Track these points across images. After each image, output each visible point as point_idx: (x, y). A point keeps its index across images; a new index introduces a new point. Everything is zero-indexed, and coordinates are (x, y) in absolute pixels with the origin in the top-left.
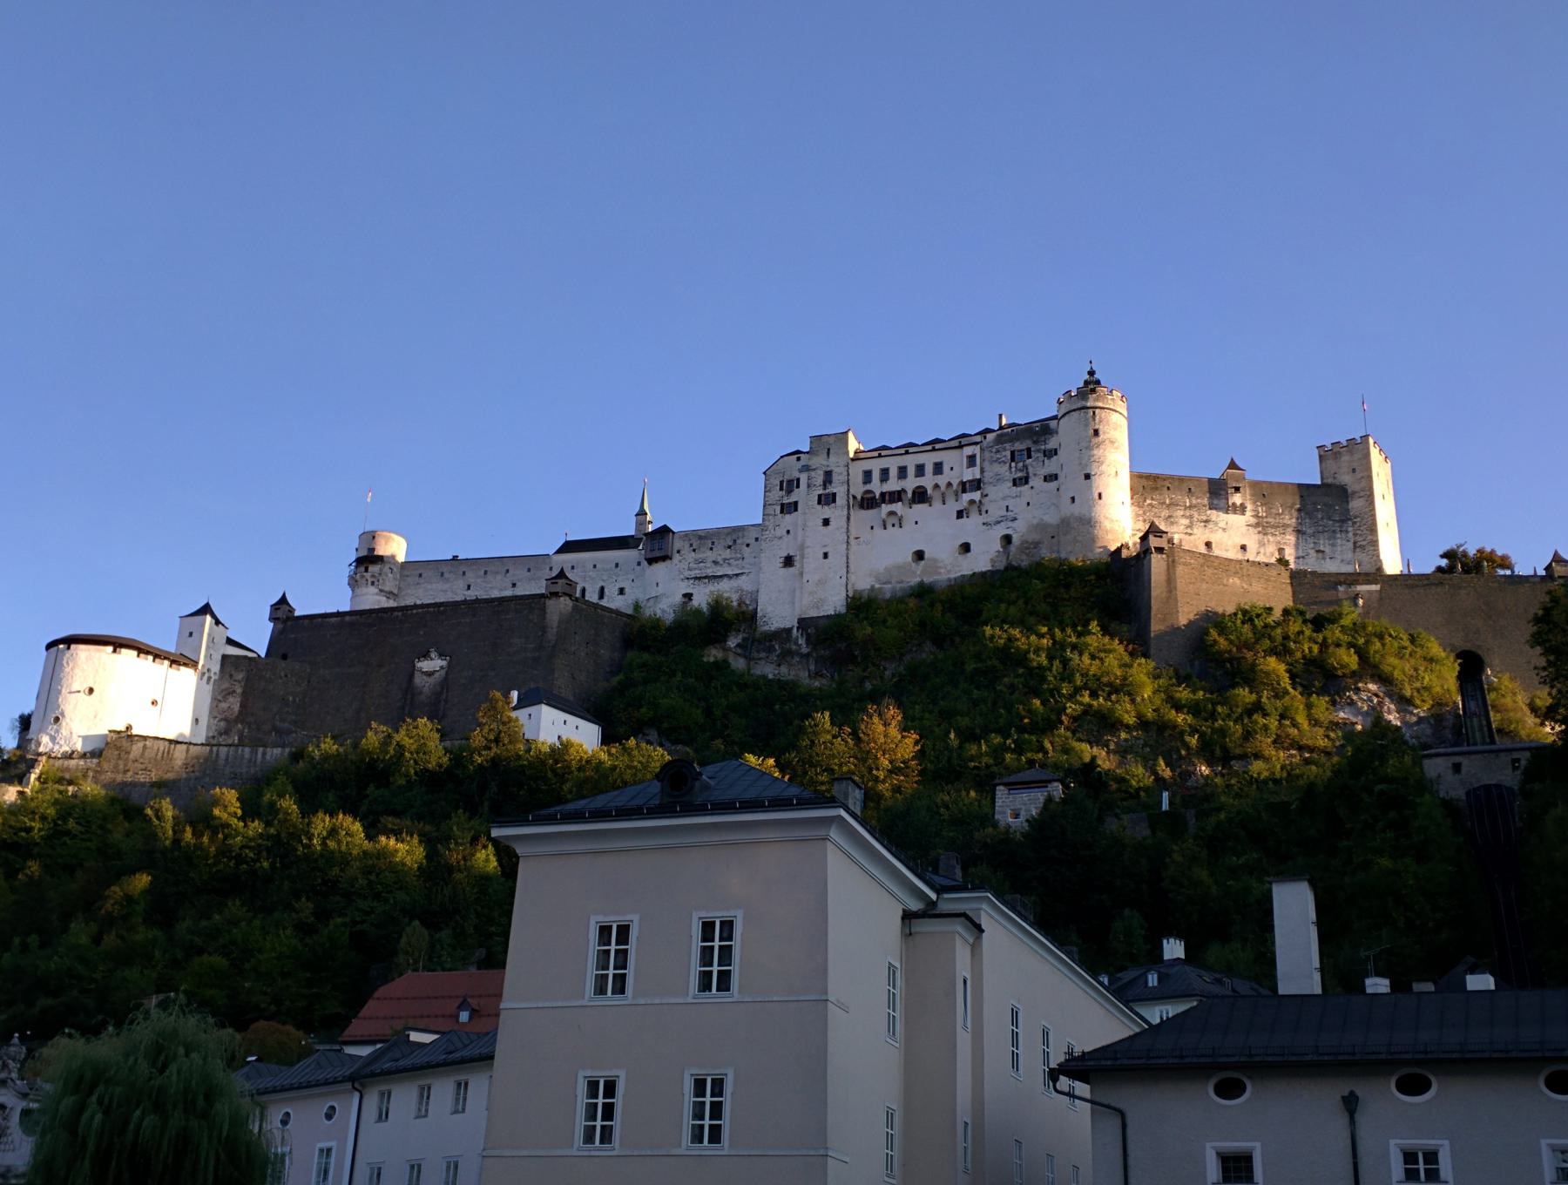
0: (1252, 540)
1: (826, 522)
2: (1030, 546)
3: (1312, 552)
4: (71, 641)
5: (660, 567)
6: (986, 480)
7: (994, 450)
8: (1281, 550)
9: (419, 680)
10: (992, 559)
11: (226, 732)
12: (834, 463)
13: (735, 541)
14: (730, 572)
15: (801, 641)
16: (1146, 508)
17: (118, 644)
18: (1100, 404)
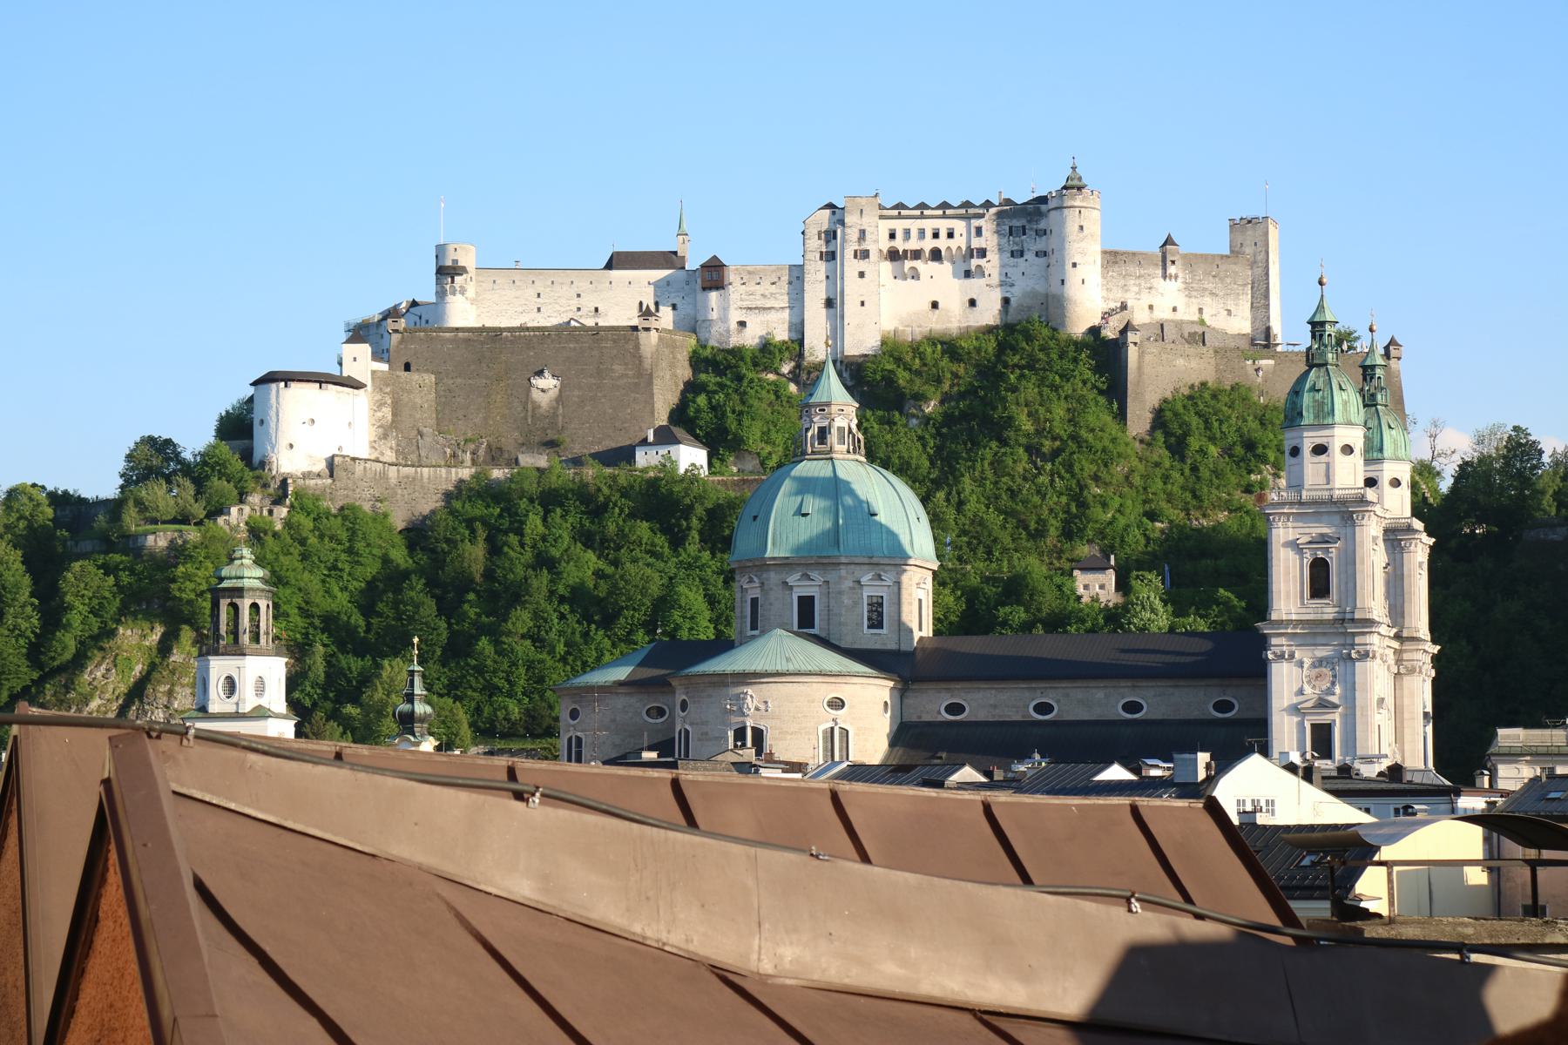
0: (1180, 300)
1: (862, 275)
3: (1222, 310)
4: (288, 378)
8: (1201, 310)
9: (536, 394)
11: (385, 436)
14: (776, 306)
16: (1109, 279)
17: (321, 379)
18: (1084, 204)
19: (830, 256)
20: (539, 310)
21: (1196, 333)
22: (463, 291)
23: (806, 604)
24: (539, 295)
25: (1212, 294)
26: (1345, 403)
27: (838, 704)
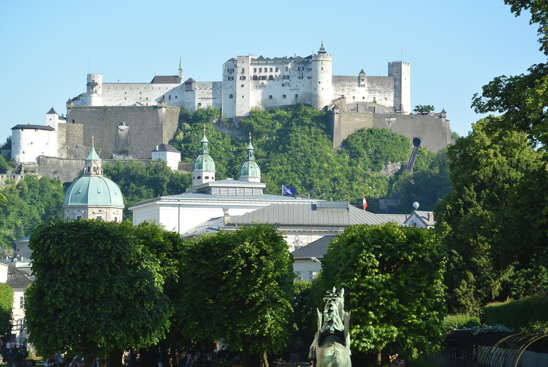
0: (366, 95)
1: (243, 86)
4: (23, 127)
5: (190, 93)
8: (374, 98)
9: (119, 132)
12: (244, 66)
18: (324, 59)
19: (232, 79)
20: (126, 99)
21: (372, 107)
22: (96, 92)
24: (126, 93)
25: (379, 92)
26: (206, 165)
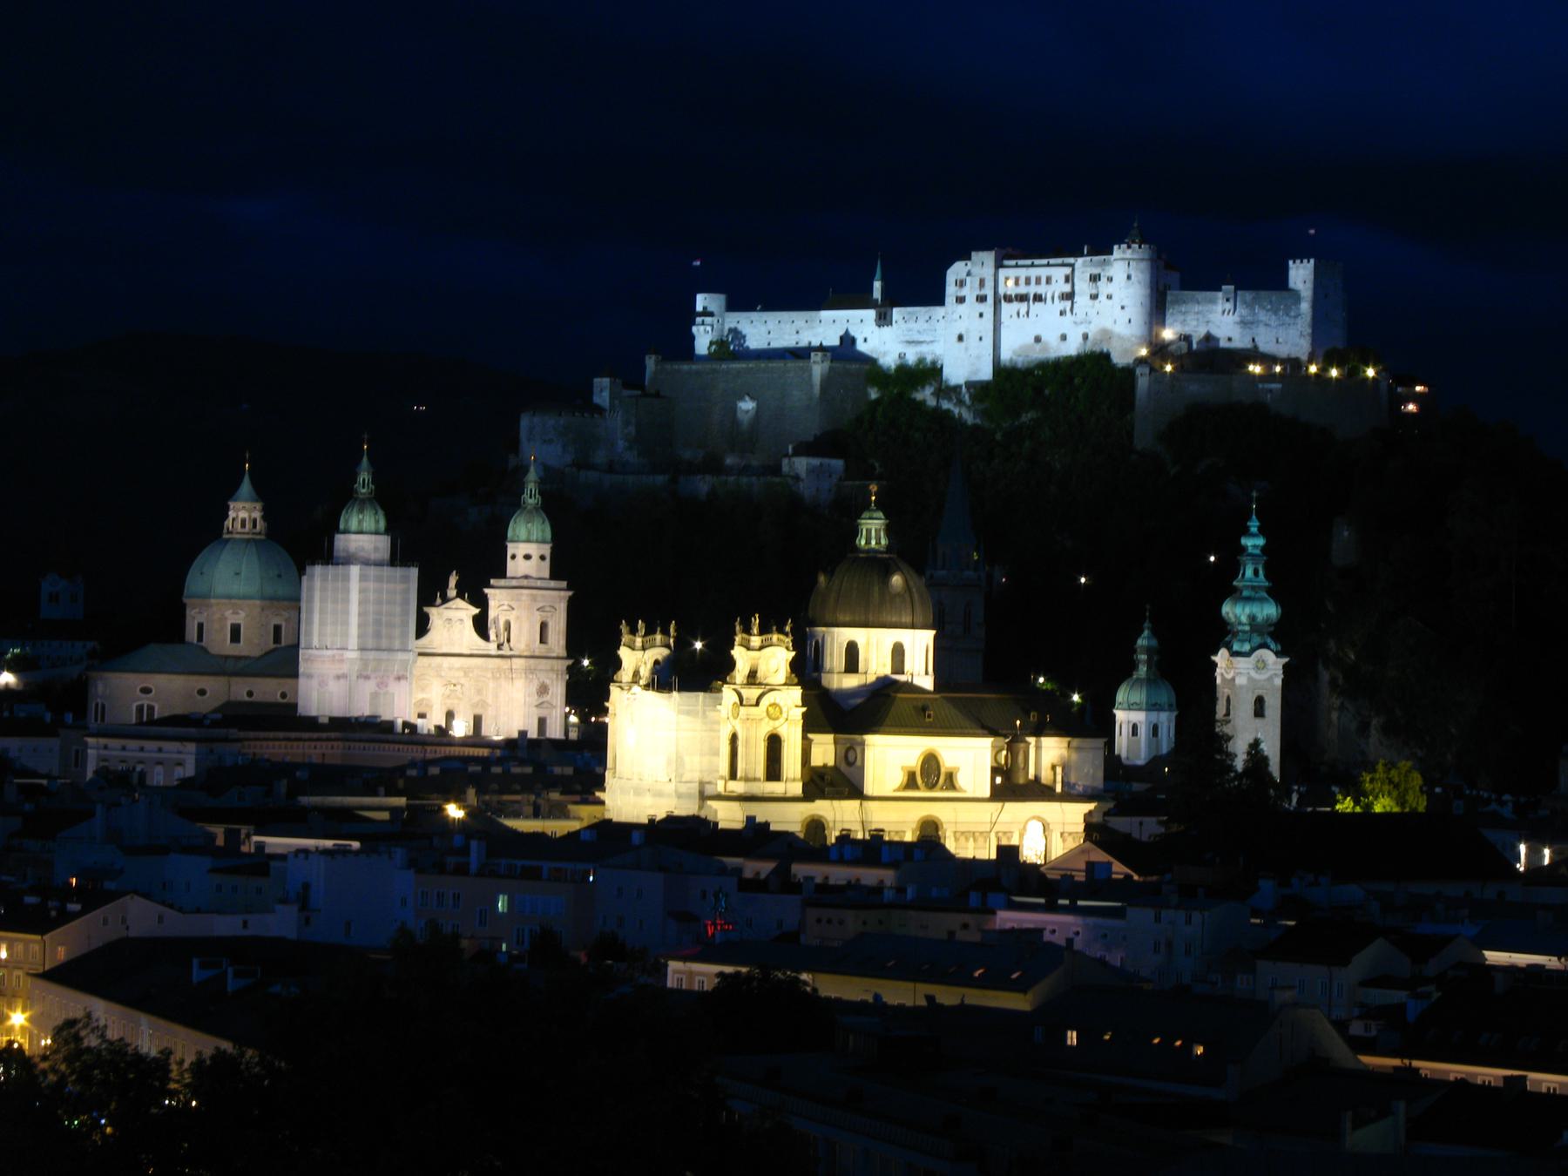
1: (981, 315)
2: (1095, 344)
6: (1076, 291)
7: (1081, 270)
8: (1253, 340)
9: (739, 415)
10: (1078, 349)
13: (930, 318)
14: (928, 339)
15: (967, 397)
18: (1135, 257)
23: (201, 626)
24: (769, 333)
25: (1267, 325)
27: (146, 691)
